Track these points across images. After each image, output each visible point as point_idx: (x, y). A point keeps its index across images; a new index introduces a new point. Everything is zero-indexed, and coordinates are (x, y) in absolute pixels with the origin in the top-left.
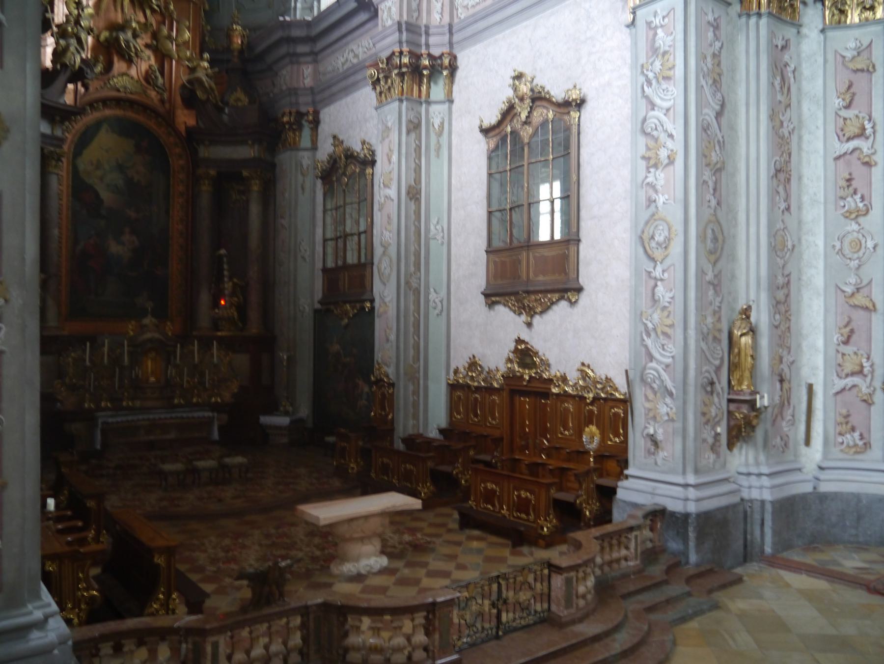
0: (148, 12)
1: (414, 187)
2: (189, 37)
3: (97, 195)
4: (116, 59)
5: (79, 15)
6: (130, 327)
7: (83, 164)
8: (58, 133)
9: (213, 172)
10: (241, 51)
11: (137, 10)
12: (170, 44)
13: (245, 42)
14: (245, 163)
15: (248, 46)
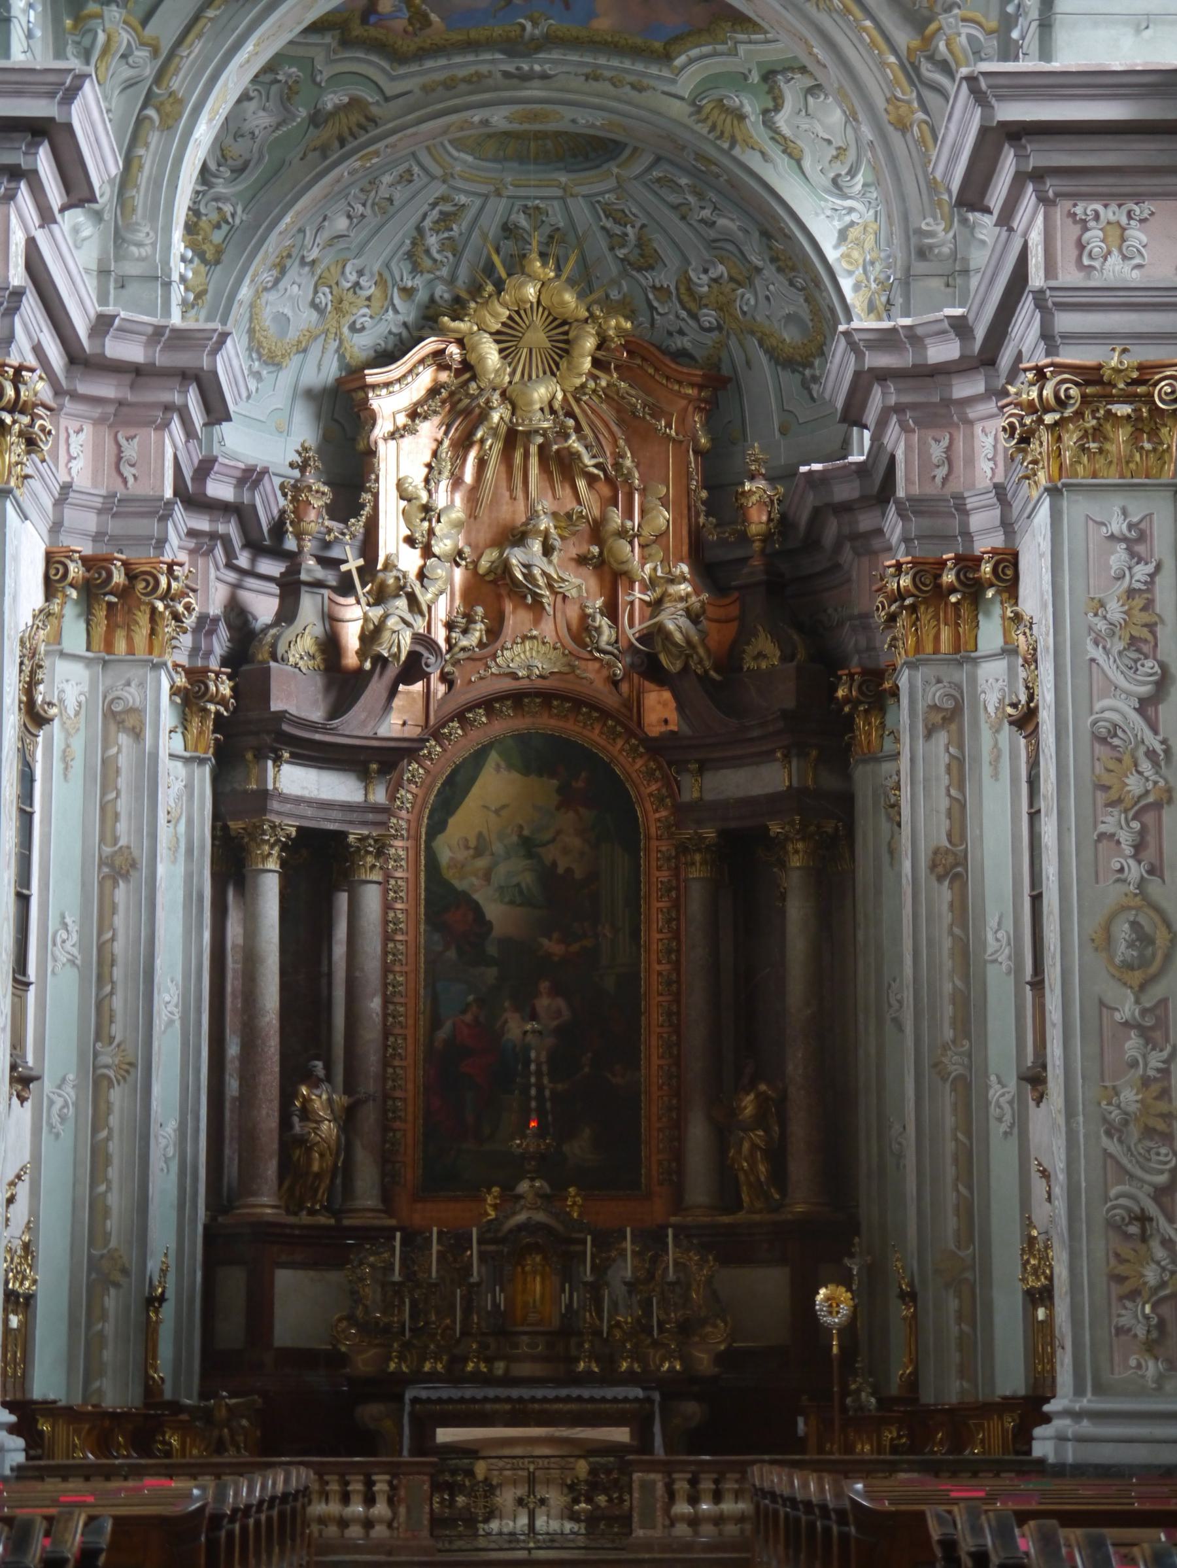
0: (581, 484)
1: (947, 851)
2: (668, 521)
3: (477, 909)
4: (509, 607)
5: (431, 532)
6: (490, 1200)
7: (448, 849)
8: (379, 795)
9: (709, 833)
10: (767, 538)
11: (558, 486)
12: (629, 548)
13: (776, 515)
14: (772, 803)
15: (783, 524)
